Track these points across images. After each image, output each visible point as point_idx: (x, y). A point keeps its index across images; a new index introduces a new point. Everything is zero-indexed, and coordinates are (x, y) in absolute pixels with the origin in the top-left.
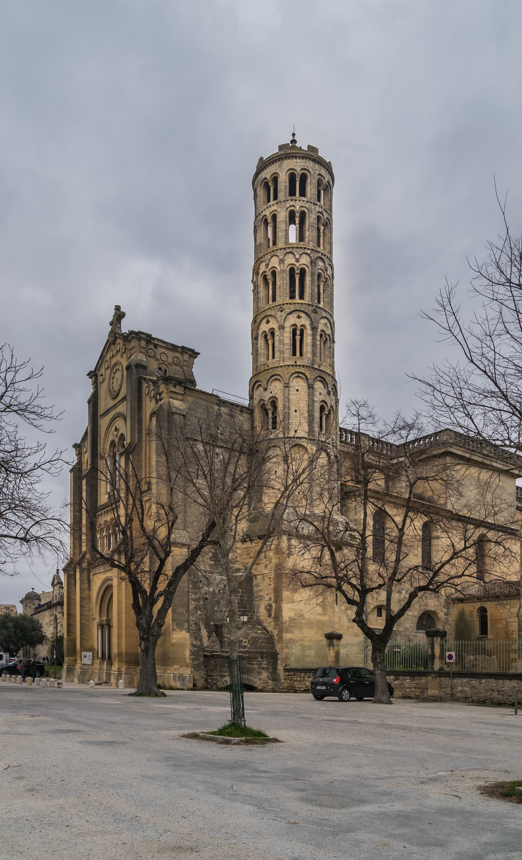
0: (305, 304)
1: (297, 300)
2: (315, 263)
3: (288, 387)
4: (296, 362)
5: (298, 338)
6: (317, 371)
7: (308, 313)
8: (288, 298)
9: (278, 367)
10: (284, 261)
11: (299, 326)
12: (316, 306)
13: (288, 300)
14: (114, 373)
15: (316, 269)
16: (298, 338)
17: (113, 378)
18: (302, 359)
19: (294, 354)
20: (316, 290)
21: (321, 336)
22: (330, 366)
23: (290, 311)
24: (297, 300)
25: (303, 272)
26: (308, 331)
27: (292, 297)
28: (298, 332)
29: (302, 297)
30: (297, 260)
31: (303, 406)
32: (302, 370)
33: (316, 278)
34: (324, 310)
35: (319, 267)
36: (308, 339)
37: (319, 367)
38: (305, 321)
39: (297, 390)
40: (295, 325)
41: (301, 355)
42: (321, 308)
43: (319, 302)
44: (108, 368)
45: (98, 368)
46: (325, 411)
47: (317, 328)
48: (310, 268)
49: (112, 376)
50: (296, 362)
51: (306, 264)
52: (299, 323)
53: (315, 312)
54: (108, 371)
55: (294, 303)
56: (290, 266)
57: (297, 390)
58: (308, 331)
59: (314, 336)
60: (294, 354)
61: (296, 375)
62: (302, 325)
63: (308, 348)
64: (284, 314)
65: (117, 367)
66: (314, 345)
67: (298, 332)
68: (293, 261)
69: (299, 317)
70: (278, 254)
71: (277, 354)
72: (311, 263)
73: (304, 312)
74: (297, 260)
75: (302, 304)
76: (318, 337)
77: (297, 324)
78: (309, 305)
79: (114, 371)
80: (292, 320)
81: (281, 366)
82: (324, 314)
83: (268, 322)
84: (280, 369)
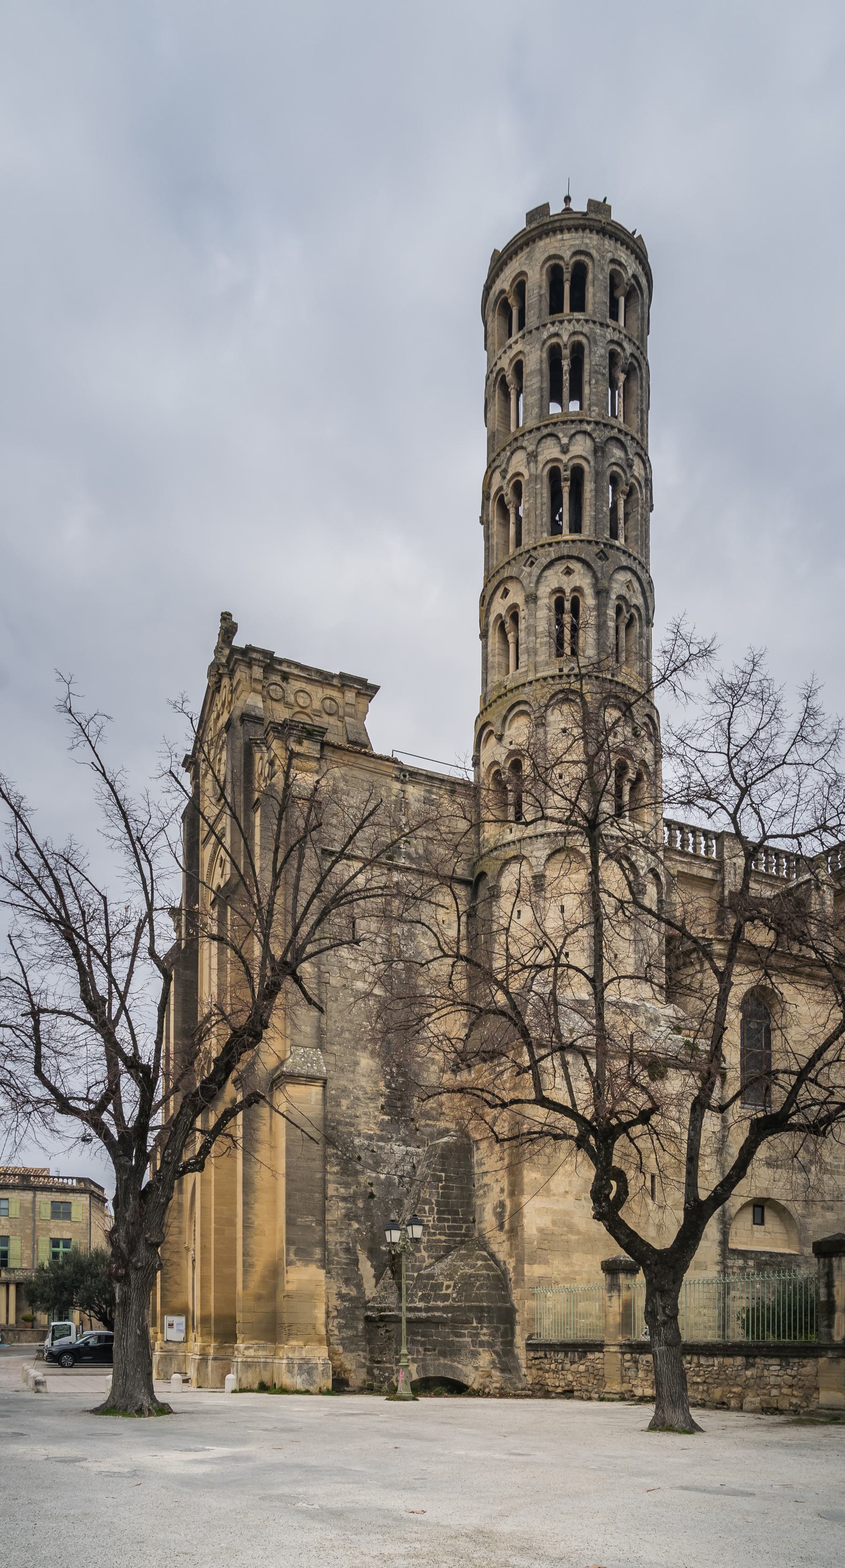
0: (582, 541)
1: (566, 535)
2: (603, 452)
3: (543, 724)
4: (561, 670)
7: (588, 559)
9: (524, 685)
10: (536, 457)
11: (568, 591)
12: (605, 544)
13: (546, 537)
15: (607, 464)
22: (641, 674)
23: (549, 560)
24: (566, 535)
25: (577, 474)
26: (589, 600)
27: (556, 529)
28: (567, 605)
29: (576, 527)
30: (565, 450)
34: (624, 552)
35: (613, 460)
37: (613, 675)
38: (581, 579)
40: (560, 590)
41: (574, 653)
42: (618, 549)
43: (614, 535)
46: (626, 773)
47: (607, 592)
48: (592, 463)
50: (561, 670)
51: (584, 454)
52: (567, 584)
53: (602, 556)
55: (558, 543)
56: (549, 466)
58: (589, 600)
59: (600, 608)
60: (559, 654)
62: (576, 589)
64: (536, 570)
67: (567, 605)
68: (555, 453)
69: (568, 572)
70: (525, 444)
71: (523, 658)
72: (595, 451)
73: (579, 559)
74: (565, 450)
75: (573, 541)
76: (611, 613)
77: (564, 587)
78: (589, 542)
80: (554, 579)
81: (530, 683)
82: (624, 561)
84: (527, 689)
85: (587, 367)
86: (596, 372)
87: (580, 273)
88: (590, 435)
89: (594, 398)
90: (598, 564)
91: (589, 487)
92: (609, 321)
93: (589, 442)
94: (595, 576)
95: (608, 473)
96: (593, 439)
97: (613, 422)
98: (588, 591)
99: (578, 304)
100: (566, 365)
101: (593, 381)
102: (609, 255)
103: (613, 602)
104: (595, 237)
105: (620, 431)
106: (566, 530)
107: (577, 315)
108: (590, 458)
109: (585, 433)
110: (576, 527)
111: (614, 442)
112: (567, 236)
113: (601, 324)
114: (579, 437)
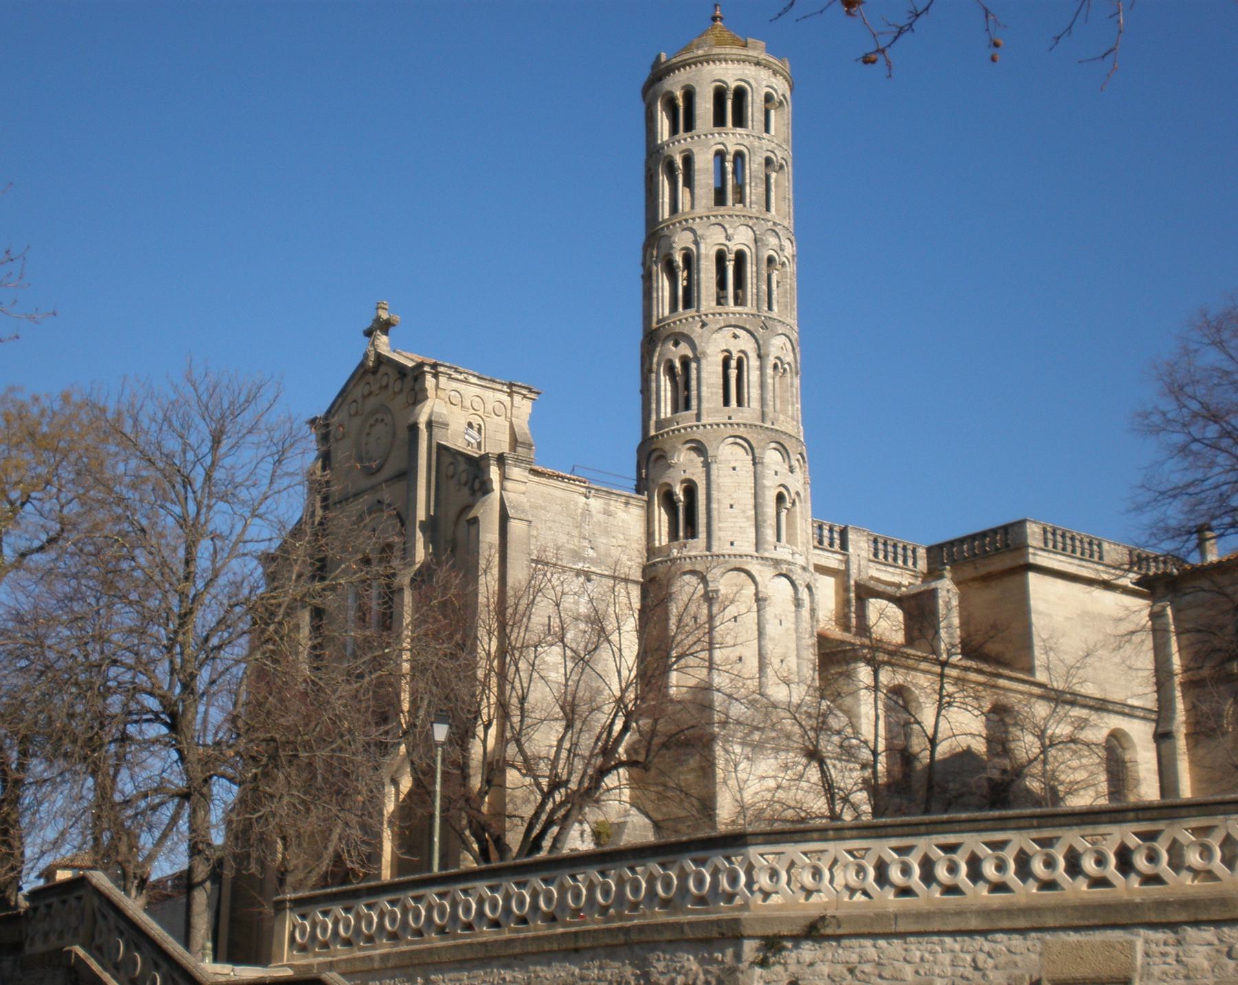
4: (730, 418)
5: (733, 373)
6: (769, 433)
7: (752, 329)
8: (714, 303)
14: (372, 425)
16: (733, 373)
17: (368, 434)
18: (742, 412)
19: (726, 402)
20: (764, 287)
21: (775, 366)
25: (740, 258)
26: (754, 362)
27: (721, 300)
28: (733, 363)
29: (739, 301)
30: (728, 238)
31: (746, 498)
32: (742, 431)
33: (764, 266)
36: (752, 376)
38: (745, 343)
39: (734, 469)
44: (357, 413)
45: (333, 411)
49: (367, 430)
50: (730, 418)
52: (735, 347)
54: (357, 421)
57: (734, 469)
58: (754, 362)
59: (762, 368)
60: (726, 402)
61: (731, 440)
62: (742, 351)
63: (753, 392)
65: (379, 416)
66: (762, 385)
67: (733, 363)
69: (735, 336)
76: (770, 371)
79: (372, 421)
83: (676, 344)
85: (747, 171)
86: (756, 177)
87: (740, 94)
88: (751, 228)
89: (753, 198)
90: (760, 332)
91: (750, 269)
92: (765, 135)
93: (750, 233)
94: (757, 341)
95: (766, 257)
96: (754, 231)
97: (769, 216)
98: (753, 356)
99: (740, 121)
100: (729, 166)
101: (753, 184)
102: (765, 83)
103: (771, 361)
104: (753, 68)
105: (775, 224)
106: (731, 301)
107: (739, 130)
108: (751, 246)
109: (748, 226)
110: (739, 301)
111: (770, 232)
112: (730, 65)
113: (759, 138)
114: (743, 228)
